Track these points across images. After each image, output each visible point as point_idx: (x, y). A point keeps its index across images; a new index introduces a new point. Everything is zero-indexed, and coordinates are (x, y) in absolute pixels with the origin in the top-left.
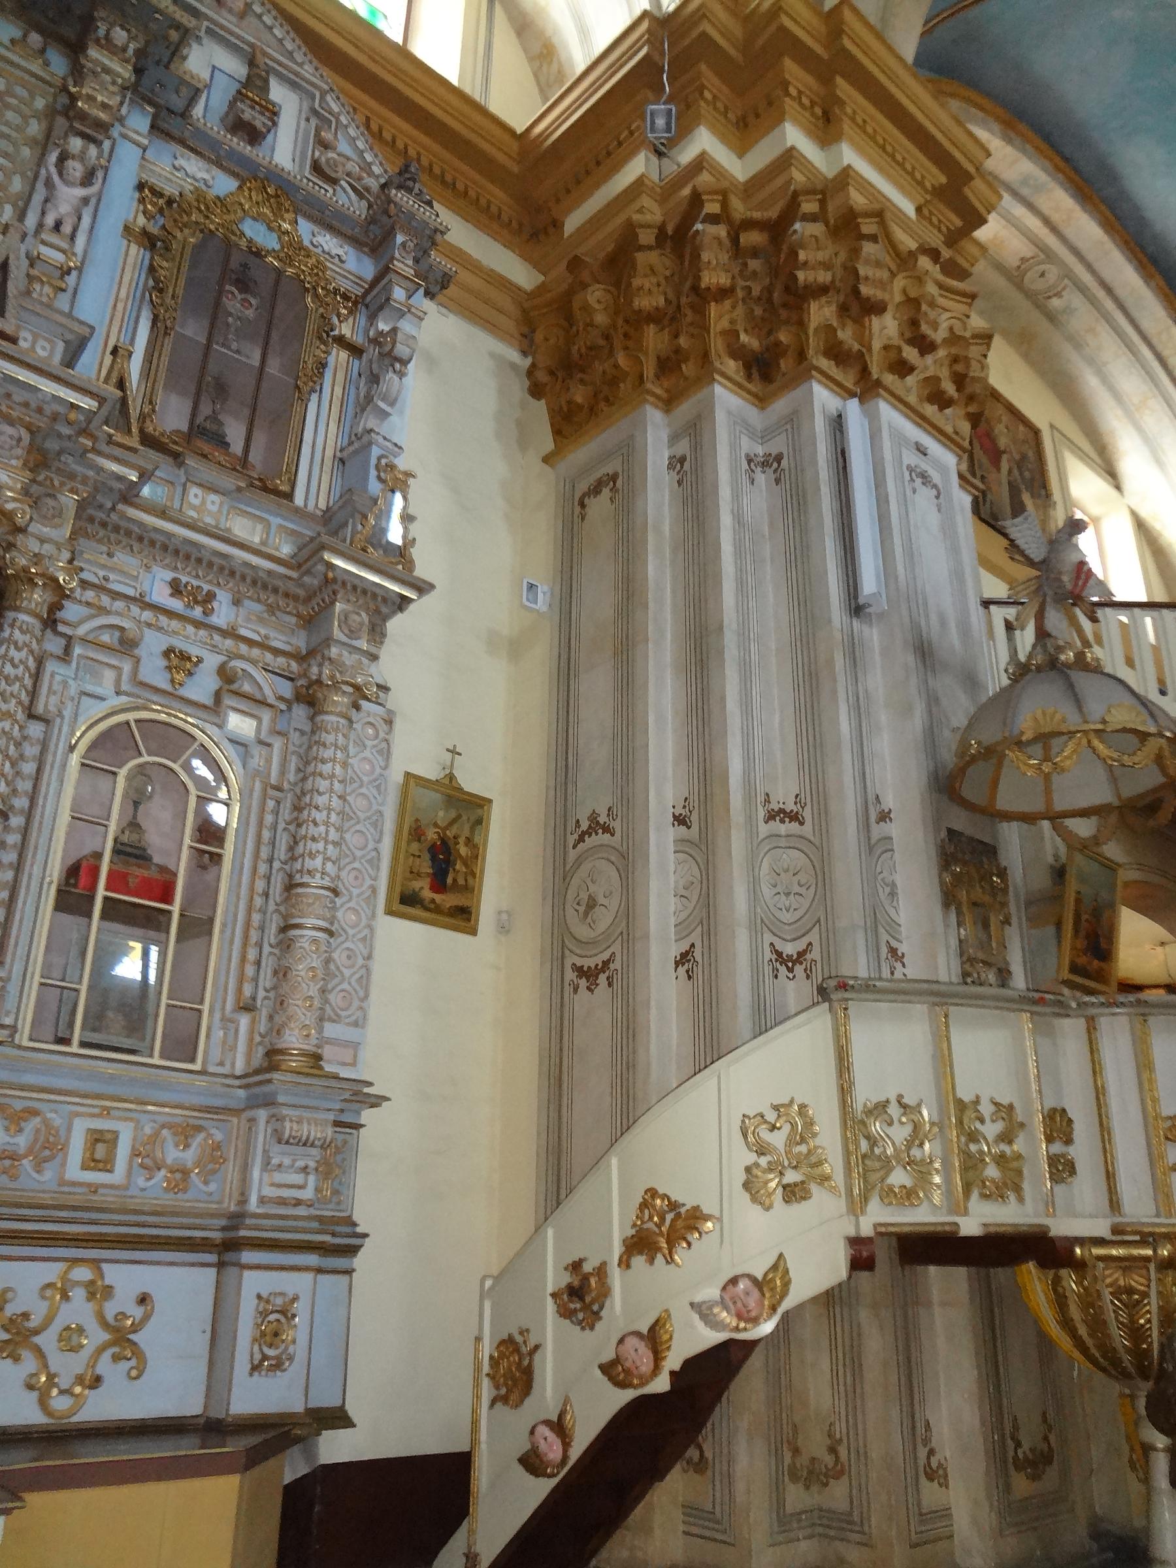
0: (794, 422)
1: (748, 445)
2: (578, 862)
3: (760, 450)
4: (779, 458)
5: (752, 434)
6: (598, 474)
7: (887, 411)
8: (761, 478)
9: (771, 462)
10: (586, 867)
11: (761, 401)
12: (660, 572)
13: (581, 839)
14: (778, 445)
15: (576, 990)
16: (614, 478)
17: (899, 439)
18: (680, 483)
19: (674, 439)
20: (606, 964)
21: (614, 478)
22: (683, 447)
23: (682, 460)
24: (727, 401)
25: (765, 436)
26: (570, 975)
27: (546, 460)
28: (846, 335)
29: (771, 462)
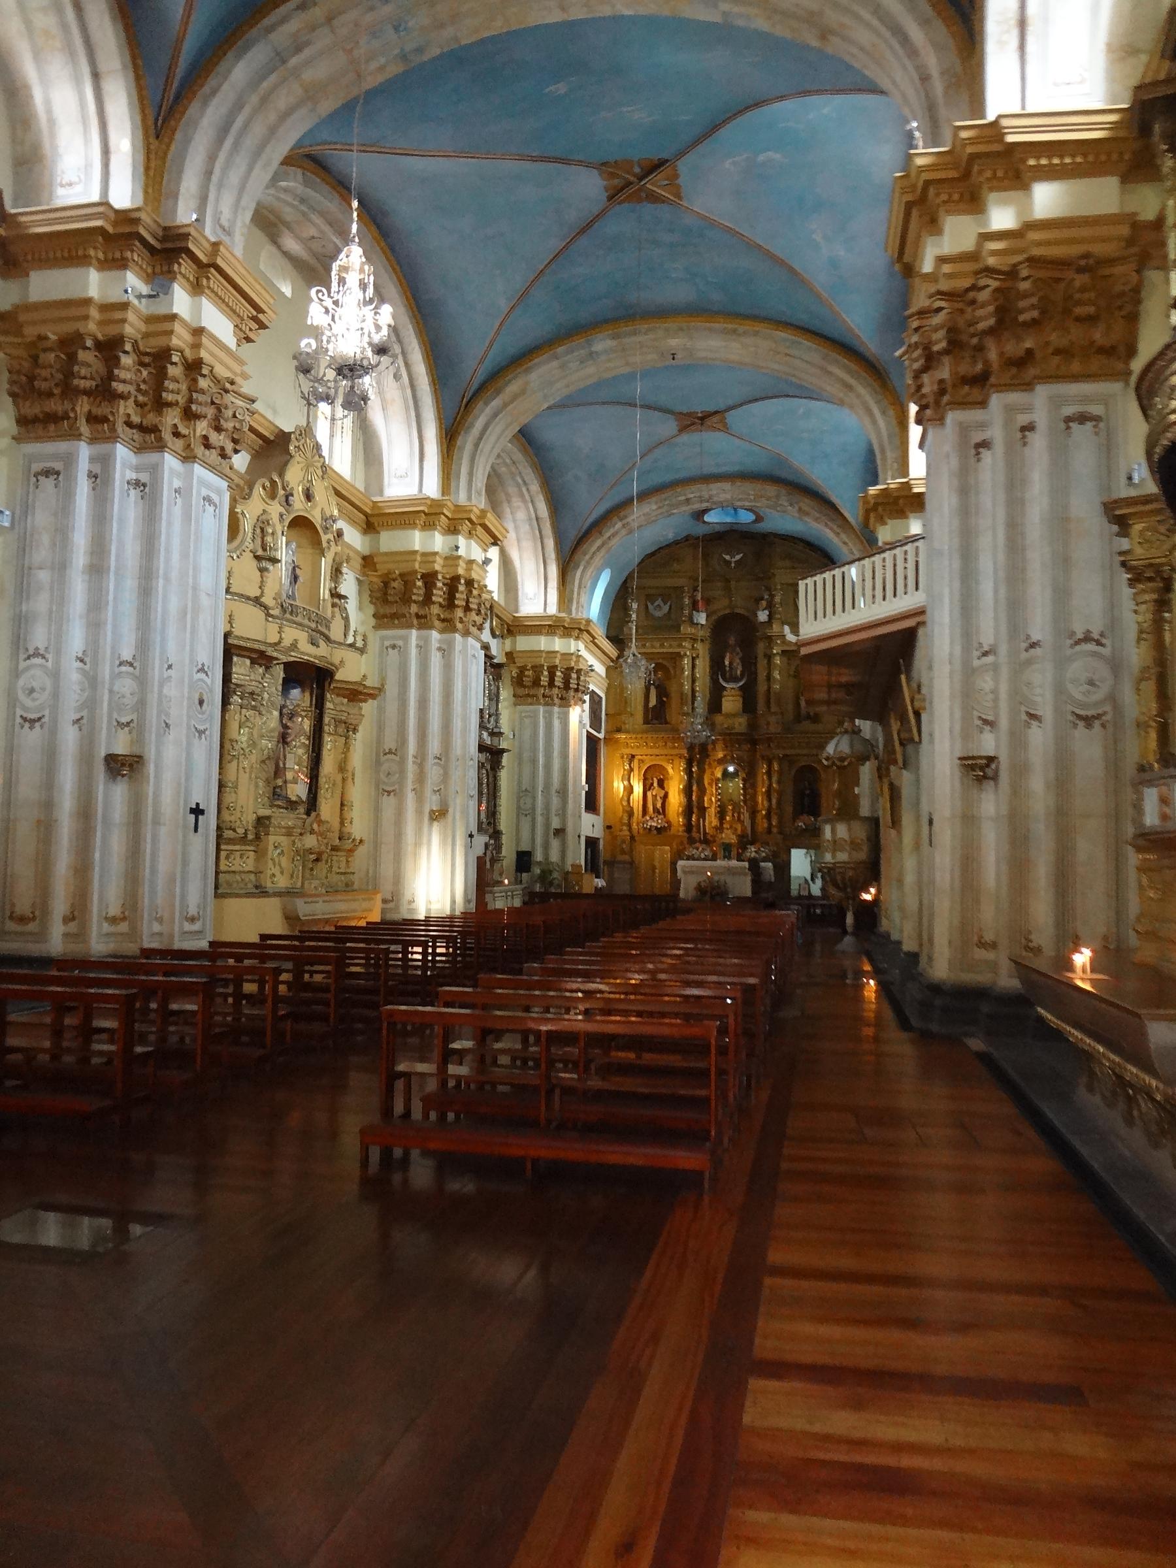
0: (155, 470)
1: (131, 475)
2: (27, 669)
3: (134, 476)
4: (144, 485)
5: (131, 468)
6: (48, 465)
7: (198, 469)
8: (132, 492)
9: (137, 484)
10: (32, 672)
11: (139, 449)
12: (80, 539)
13: (29, 658)
14: (144, 477)
15: (22, 727)
16: (58, 473)
17: (202, 482)
18: (94, 489)
19: (92, 460)
20: (39, 719)
21: (58, 473)
22: (97, 469)
23: (96, 477)
24: (122, 453)
25: (138, 469)
26: (19, 720)
27: (13, 438)
28: (183, 430)
29: (137, 484)
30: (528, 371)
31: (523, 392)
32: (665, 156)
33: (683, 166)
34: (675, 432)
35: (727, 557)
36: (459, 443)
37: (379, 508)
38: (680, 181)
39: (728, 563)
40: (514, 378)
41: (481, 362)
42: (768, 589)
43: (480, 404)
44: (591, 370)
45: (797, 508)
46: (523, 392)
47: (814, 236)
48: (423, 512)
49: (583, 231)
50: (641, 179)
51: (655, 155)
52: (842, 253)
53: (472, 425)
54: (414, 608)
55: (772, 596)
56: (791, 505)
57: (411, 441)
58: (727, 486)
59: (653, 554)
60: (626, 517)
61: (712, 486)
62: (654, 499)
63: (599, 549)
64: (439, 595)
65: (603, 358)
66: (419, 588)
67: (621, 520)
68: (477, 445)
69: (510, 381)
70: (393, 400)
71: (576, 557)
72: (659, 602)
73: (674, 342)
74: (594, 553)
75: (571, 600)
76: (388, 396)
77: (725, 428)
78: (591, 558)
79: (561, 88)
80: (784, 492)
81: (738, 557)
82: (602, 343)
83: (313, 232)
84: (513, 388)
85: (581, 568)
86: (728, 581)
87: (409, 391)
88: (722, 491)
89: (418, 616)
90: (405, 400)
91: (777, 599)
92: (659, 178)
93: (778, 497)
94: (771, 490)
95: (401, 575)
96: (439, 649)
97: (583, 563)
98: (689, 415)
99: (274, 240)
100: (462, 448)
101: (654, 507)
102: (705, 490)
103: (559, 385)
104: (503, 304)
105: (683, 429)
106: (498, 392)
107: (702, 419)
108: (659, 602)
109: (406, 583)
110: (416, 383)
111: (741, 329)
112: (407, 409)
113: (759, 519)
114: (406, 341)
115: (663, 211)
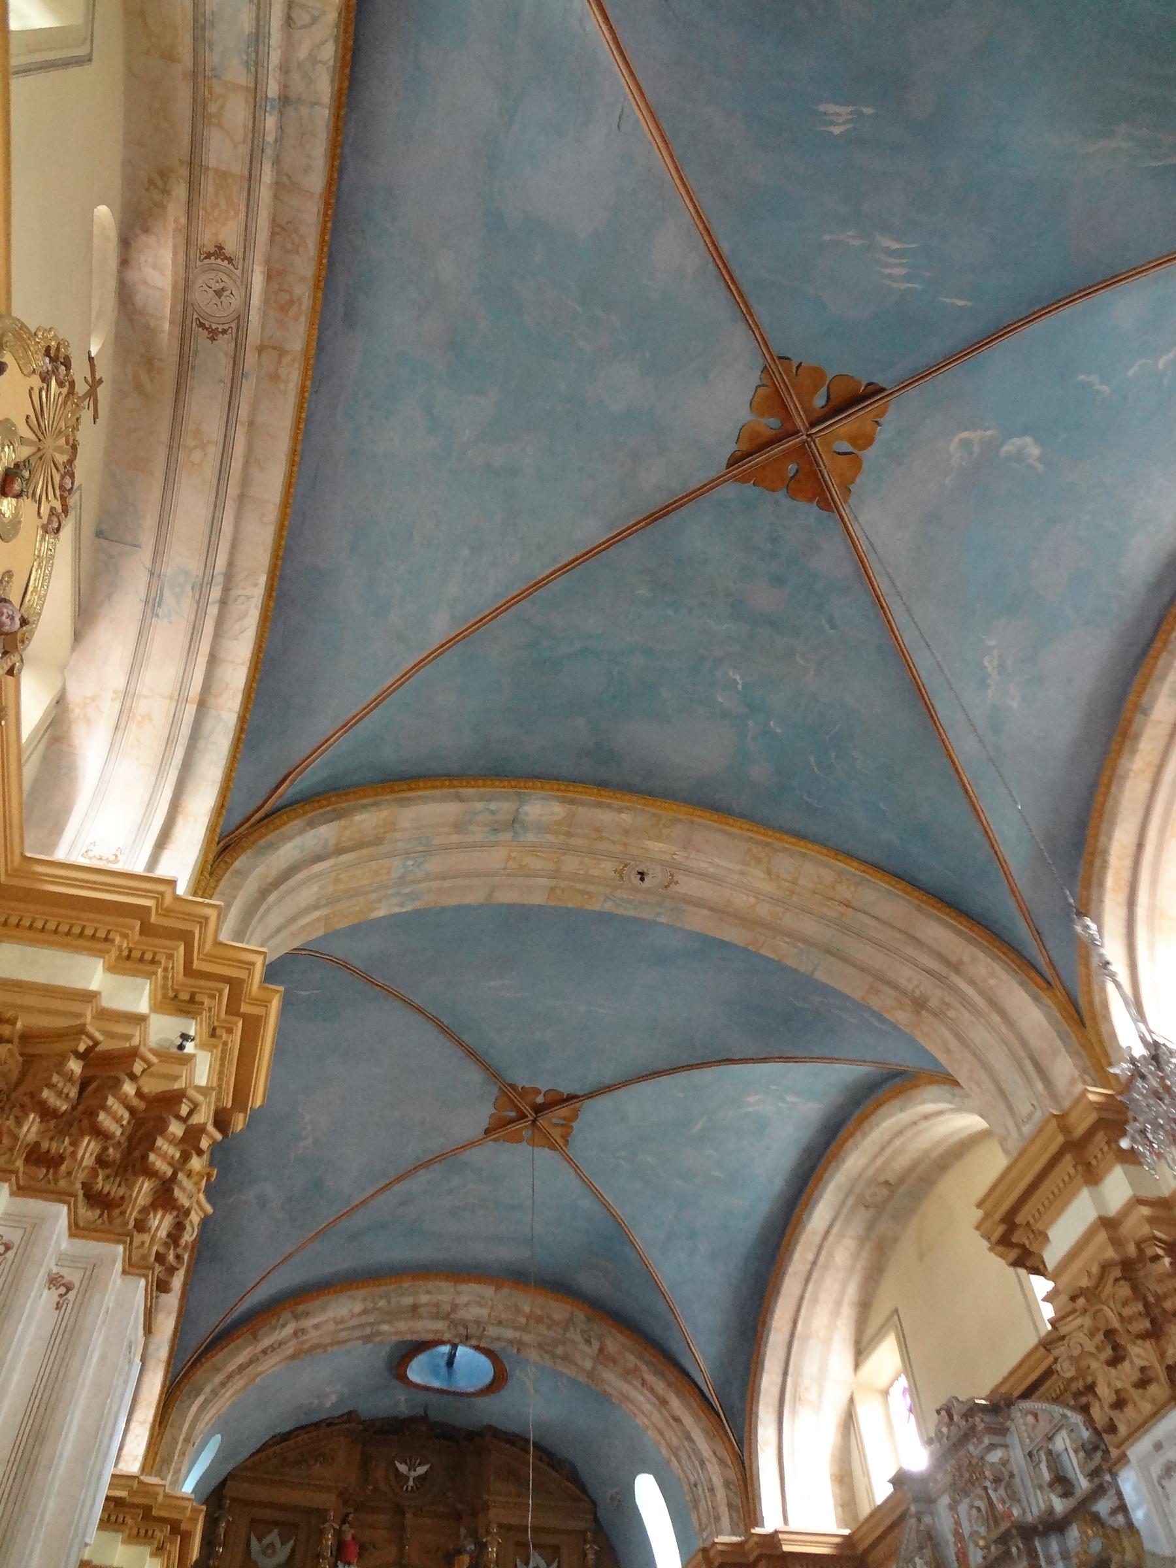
30: (407, 802)
31: (378, 841)
32: (879, 380)
33: (893, 420)
34: (480, 1133)
35: (402, 1468)
36: (237, 864)
37: (38, 877)
38: (869, 455)
39: (402, 1478)
40: (375, 804)
41: (347, 726)
42: (473, 1534)
43: (298, 823)
44: (496, 858)
45: (596, 1345)
46: (378, 841)
47: (986, 662)
48: (141, 913)
49: (654, 517)
50: (812, 425)
51: (864, 376)
52: (1014, 704)
53: (271, 846)
54: (31, 1128)
55: (482, 1547)
56: (588, 1342)
57: (150, 805)
58: (488, 1291)
59: (284, 1437)
60: (307, 1314)
61: (463, 1287)
62: (363, 1292)
63: (241, 1368)
64: (114, 1119)
65: (530, 837)
66: (70, 1078)
67: (297, 1317)
68: (264, 893)
69: (364, 807)
70: (148, 717)
71: (199, 1375)
72: (273, 1537)
73: (655, 847)
74: (230, 1377)
75: (167, 1461)
76: (141, 707)
77: (559, 1143)
78: (223, 1384)
79: (839, 117)
80: (580, 1315)
81: (422, 1470)
82: (542, 809)
83: (230, 235)
84: (367, 820)
85: (201, 1399)
86: (400, 1511)
87: (191, 709)
88: (474, 1302)
89: (37, 1157)
90: (175, 721)
91: (492, 1551)
92: (846, 425)
93: (569, 1322)
94: (559, 1310)
95: (26, 1038)
96: (54, 1281)
97: (208, 1389)
98: (524, 1093)
99: (135, 225)
100: (242, 874)
101: (358, 1307)
102: (443, 1293)
103: (434, 865)
104: (441, 627)
105: (496, 1128)
106: (339, 815)
107: (539, 1109)
108: (273, 1537)
109: (29, 1060)
110: (211, 701)
111: (777, 844)
112: (170, 741)
113: (500, 1379)
114: (236, 609)
115: (809, 512)
